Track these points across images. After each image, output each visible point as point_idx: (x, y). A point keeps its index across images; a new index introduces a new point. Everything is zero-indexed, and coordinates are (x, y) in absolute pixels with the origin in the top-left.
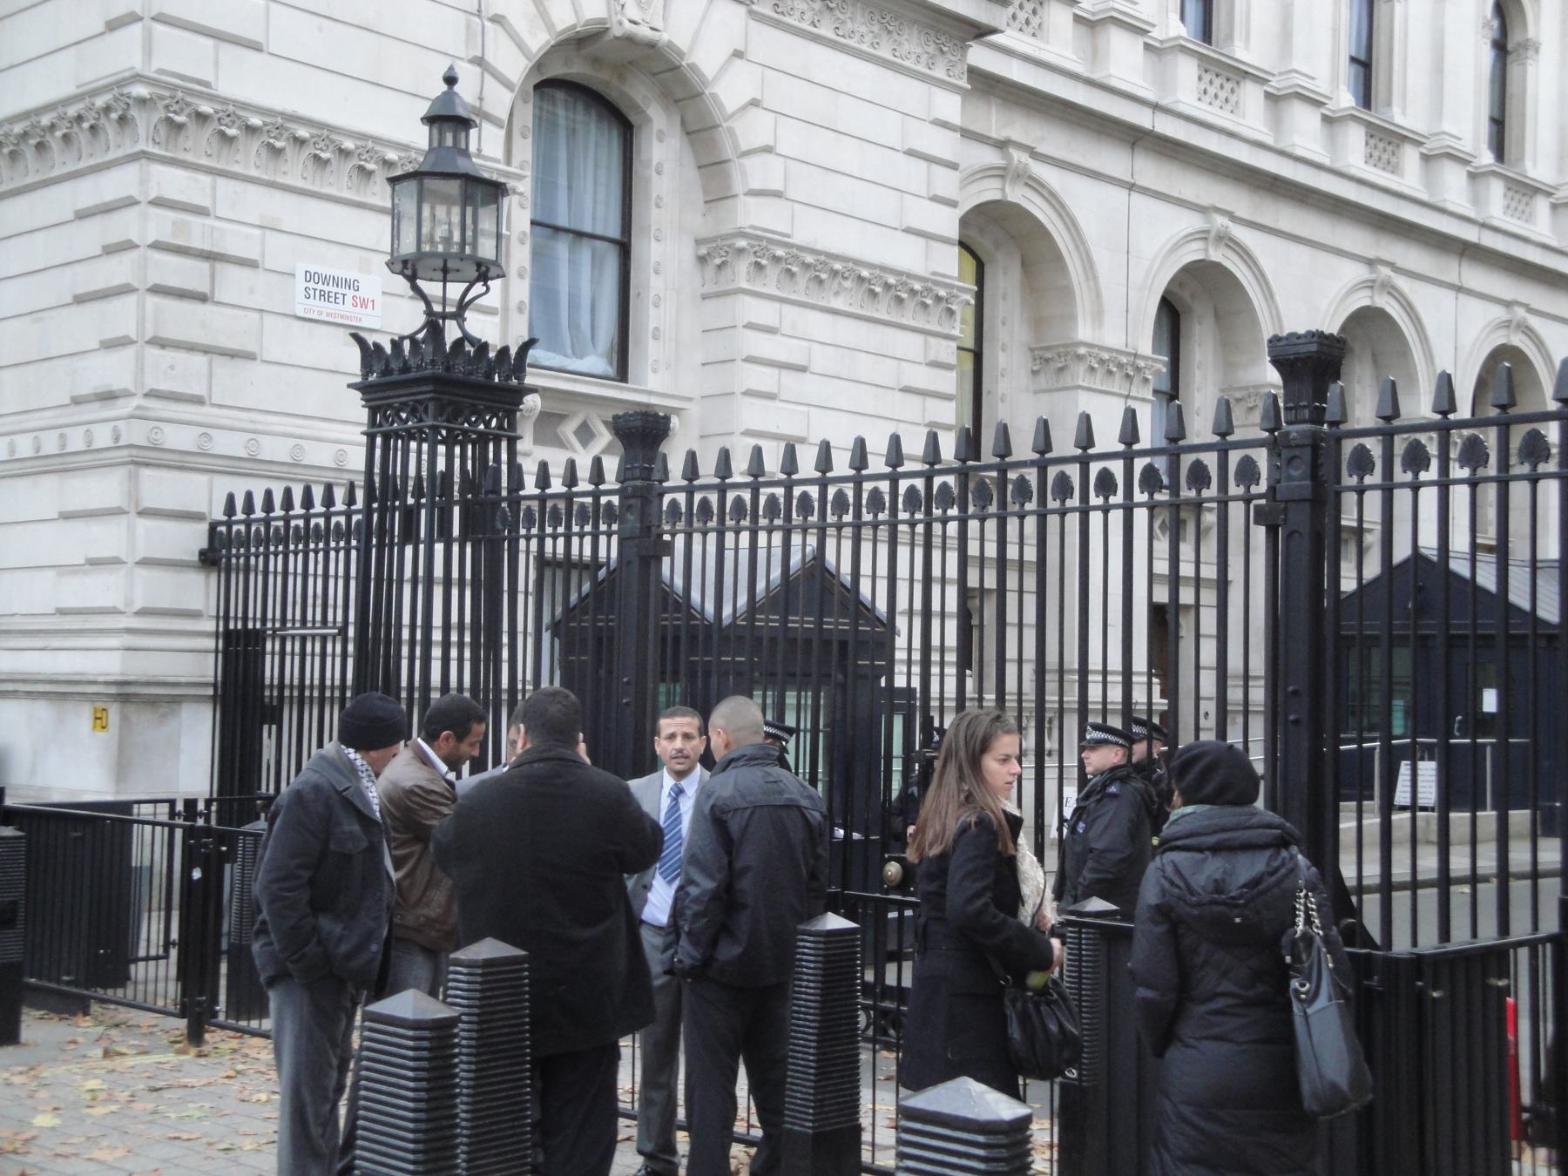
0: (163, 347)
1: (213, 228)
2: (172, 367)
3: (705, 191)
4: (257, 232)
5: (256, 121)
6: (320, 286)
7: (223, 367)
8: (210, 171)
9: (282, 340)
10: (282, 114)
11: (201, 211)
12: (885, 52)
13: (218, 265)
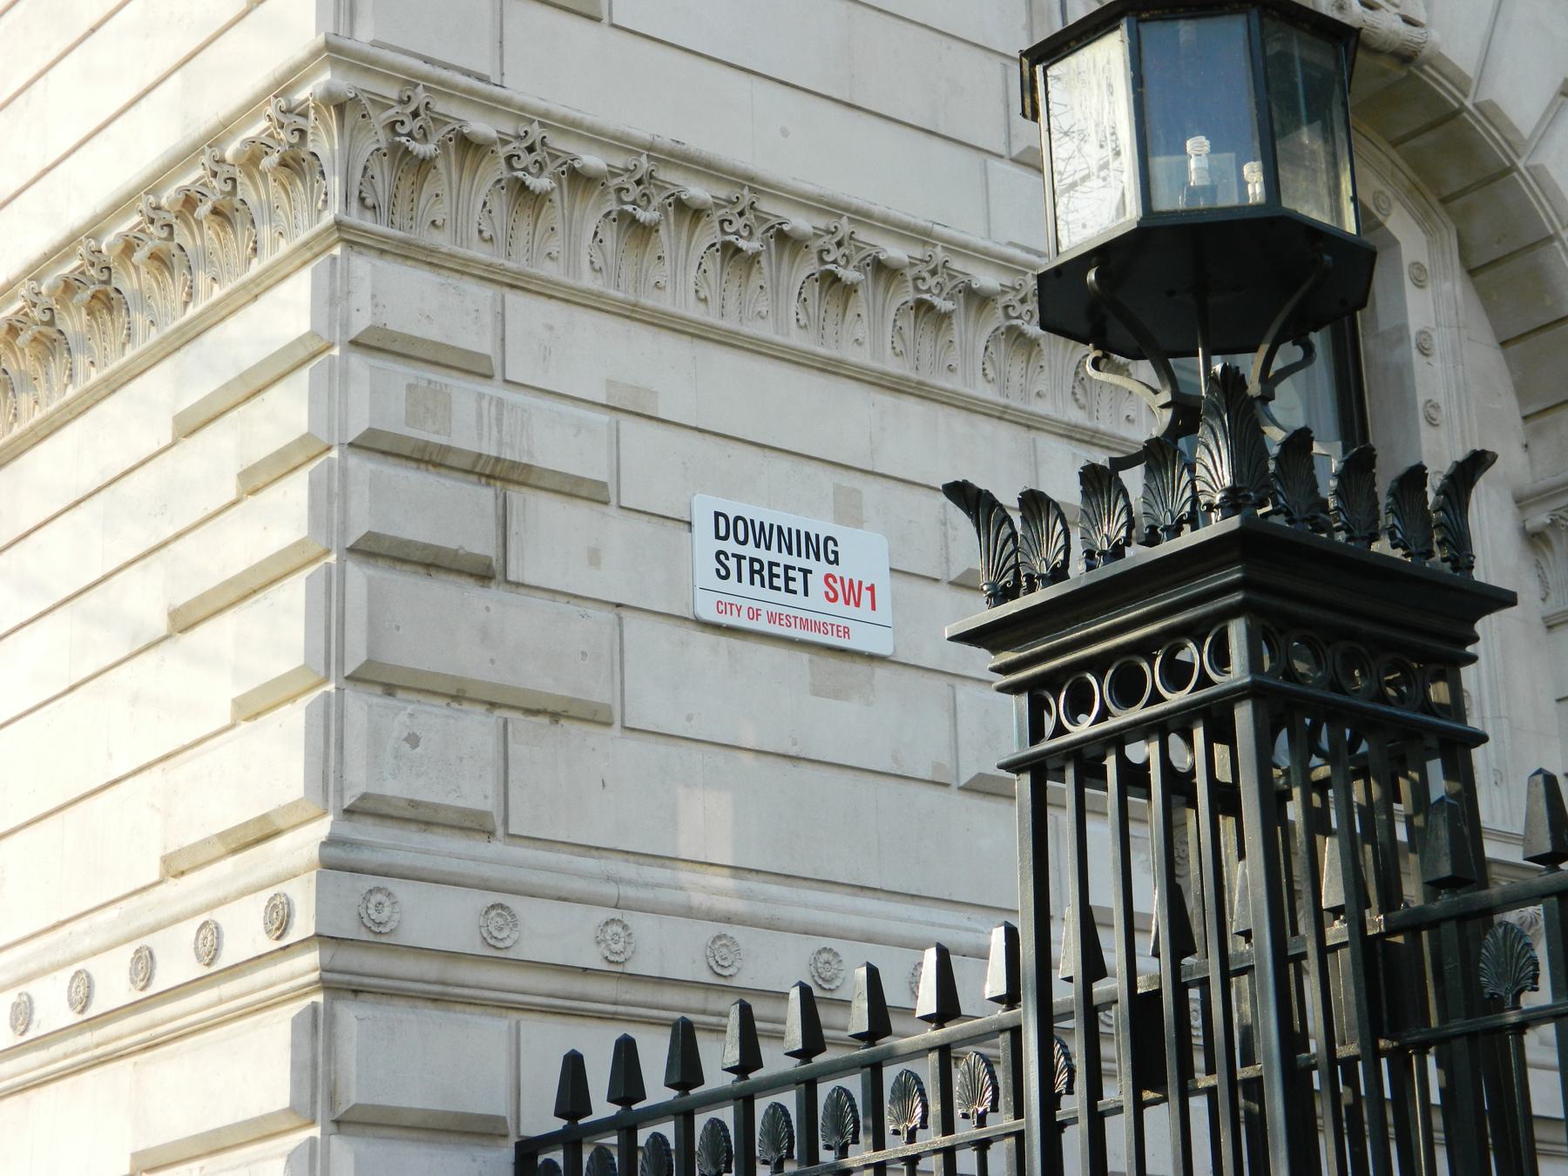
0: (390, 689)
1: (500, 403)
2: (413, 740)
3: (1522, 392)
4: (604, 418)
5: (592, 160)
6: (749, 550)
7: (536, 747)
8: (490, 276)
9: (673, 680)
10: (650, 148)
11: (475, 368)
13: (516, 495)
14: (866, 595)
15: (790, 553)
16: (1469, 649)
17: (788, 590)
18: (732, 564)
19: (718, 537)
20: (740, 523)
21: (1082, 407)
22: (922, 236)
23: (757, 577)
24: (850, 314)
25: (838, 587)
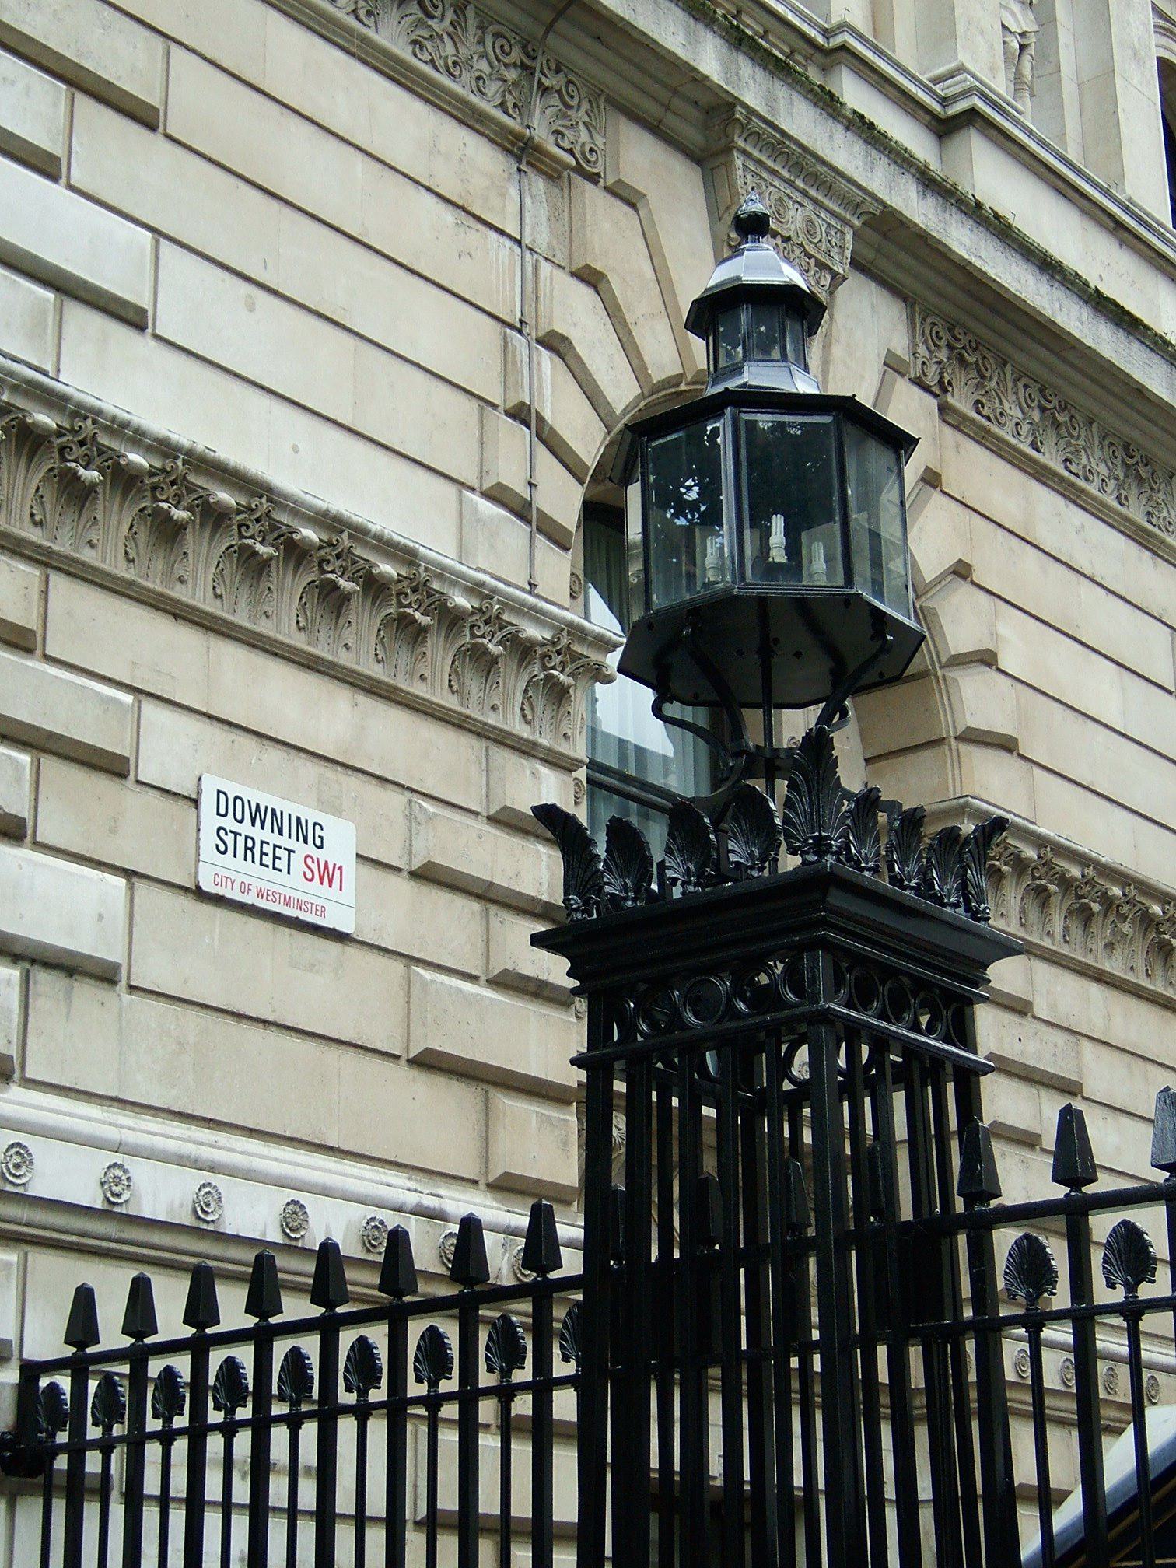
4: (128, 698)
6: (246, 828)
12: (1136, 512)
15: (281, 833)
18: (229, 839)
21: (528, 723)
22: (406, 555)
23: (249, 853)
24: (341, 622)
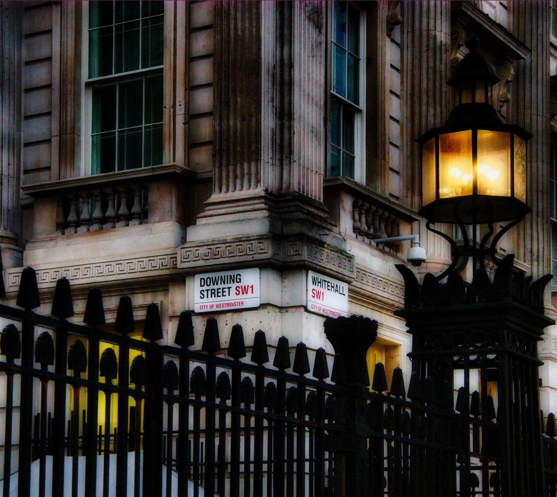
14: (250, 289)
15: (224, 283)
16: (542, 336)
17: (223, 296)
18: (205, 293)
19: (201, 286)
20: (209, 280)
23: (213, 295)
25: (240, 290)
